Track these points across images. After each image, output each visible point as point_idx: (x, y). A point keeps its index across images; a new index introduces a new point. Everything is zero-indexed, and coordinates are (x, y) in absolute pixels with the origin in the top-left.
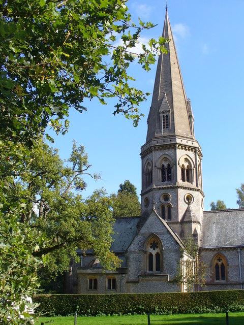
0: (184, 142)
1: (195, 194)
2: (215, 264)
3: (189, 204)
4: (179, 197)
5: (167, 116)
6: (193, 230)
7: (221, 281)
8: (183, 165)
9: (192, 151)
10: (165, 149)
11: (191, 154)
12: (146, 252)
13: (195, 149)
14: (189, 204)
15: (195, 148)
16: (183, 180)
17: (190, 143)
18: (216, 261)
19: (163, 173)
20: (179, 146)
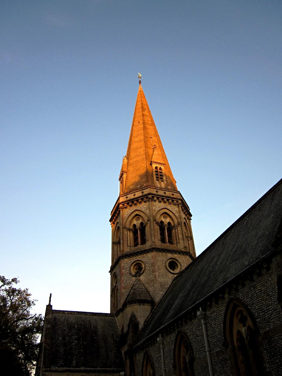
1: (147, 259)
6: (129, 316)
9: (145, 202)
11: (143, 206)
13: (147, 198)
15: (146, 196)
17: (138, 194)
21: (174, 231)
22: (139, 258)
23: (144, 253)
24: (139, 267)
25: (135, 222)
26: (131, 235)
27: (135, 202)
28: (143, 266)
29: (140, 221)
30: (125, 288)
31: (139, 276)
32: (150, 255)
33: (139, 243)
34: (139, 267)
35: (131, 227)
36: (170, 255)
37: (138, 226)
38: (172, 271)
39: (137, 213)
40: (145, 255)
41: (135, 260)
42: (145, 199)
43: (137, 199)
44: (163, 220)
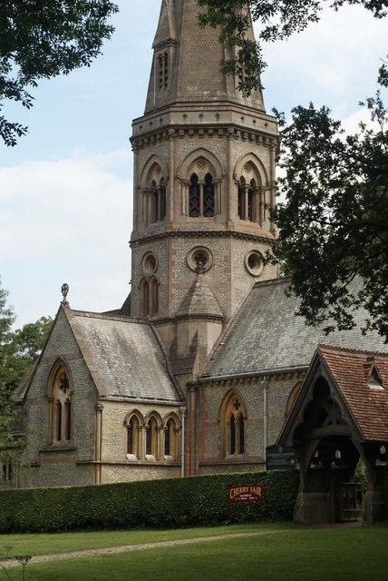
0: (193, 119)
2: (228, 415)
3: (197, 271)
4: (174, 258)
5: (166, 54)
6: (192, 335)
7: (237, 456)
8: (194, 177)
9: (220, 136)
10: (154, 143)
11: (214, 145)
12: (50, 400)
13: (225, 130)
14: (197, 271)
15: (225, 127)
16: (194, 212)
17: (209, 120)
18: (231, 409)
19: (194, 199)
20: (177, 131)
21: (257, 196)
22: (205, 243)
23: (214, 236)
24: (201, 256)
25: (196, 170)
26: (186, 192)
27: (201, 132)
28: (210, 257)
29: (206, 171)
30: (177, 287)
31: (203, 273)
32: (222, 241)
33: (202, 212)
34: (201, 256)
35: (189, 178)
36: (251, 246)
37: (201, 178)
38: (249, 268)
39: (202, 153)
40: (214, 240)
41: (196, 244)
42: (221, 132)
43: (206, 128)
44: (245, 175)
